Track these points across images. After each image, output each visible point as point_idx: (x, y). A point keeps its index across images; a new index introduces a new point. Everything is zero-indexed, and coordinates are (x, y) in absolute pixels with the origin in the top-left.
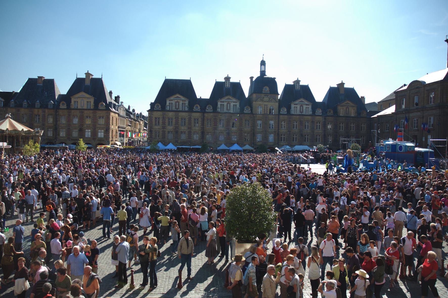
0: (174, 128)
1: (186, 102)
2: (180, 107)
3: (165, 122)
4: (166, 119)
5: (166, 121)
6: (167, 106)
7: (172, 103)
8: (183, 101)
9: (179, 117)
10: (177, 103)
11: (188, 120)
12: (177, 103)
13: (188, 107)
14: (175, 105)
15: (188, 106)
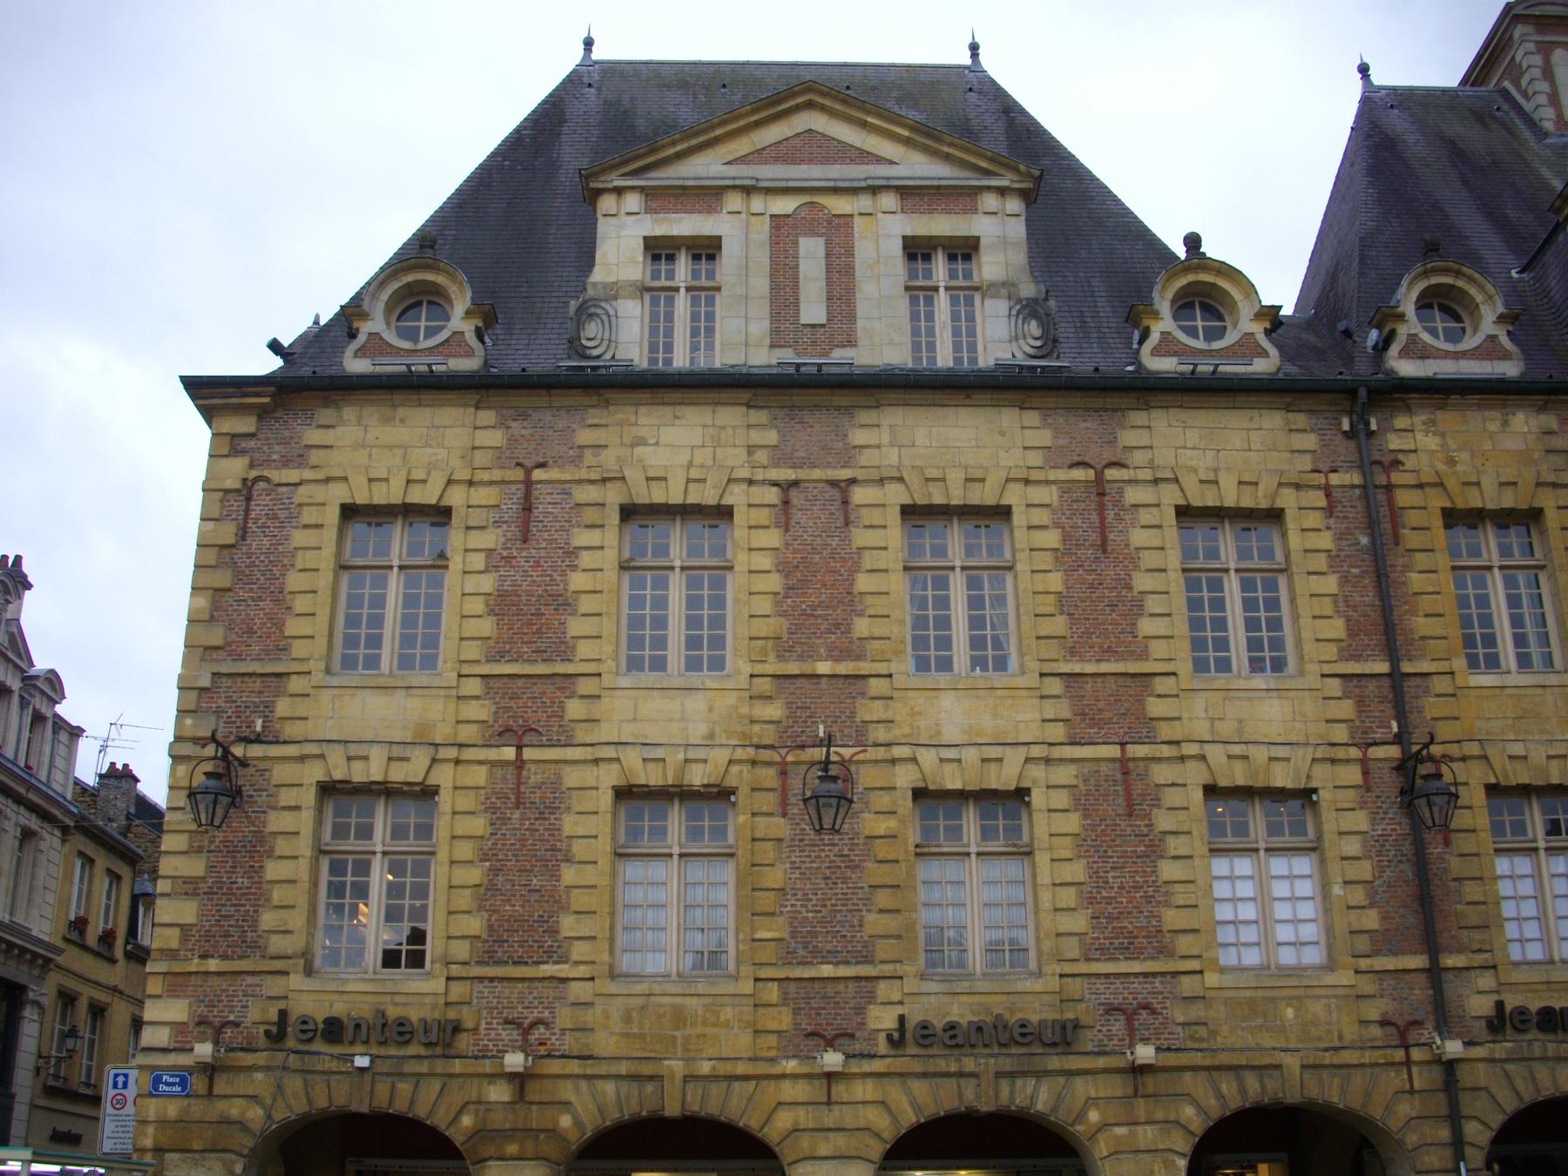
0: (774, 711)
1: (981, 226)
2: (864, 308)
3: (564, 603)
4: (582, 538)
5: (578, 581)
6: (613, 292)
7: (706, 250)
8: (912, 194)
9: (859, 495)
10: (811, 253)
11: (1052, 539)
12: (811, 253)
13: (1030, 309)
14: (761, 284)
15: (1028, 290)
